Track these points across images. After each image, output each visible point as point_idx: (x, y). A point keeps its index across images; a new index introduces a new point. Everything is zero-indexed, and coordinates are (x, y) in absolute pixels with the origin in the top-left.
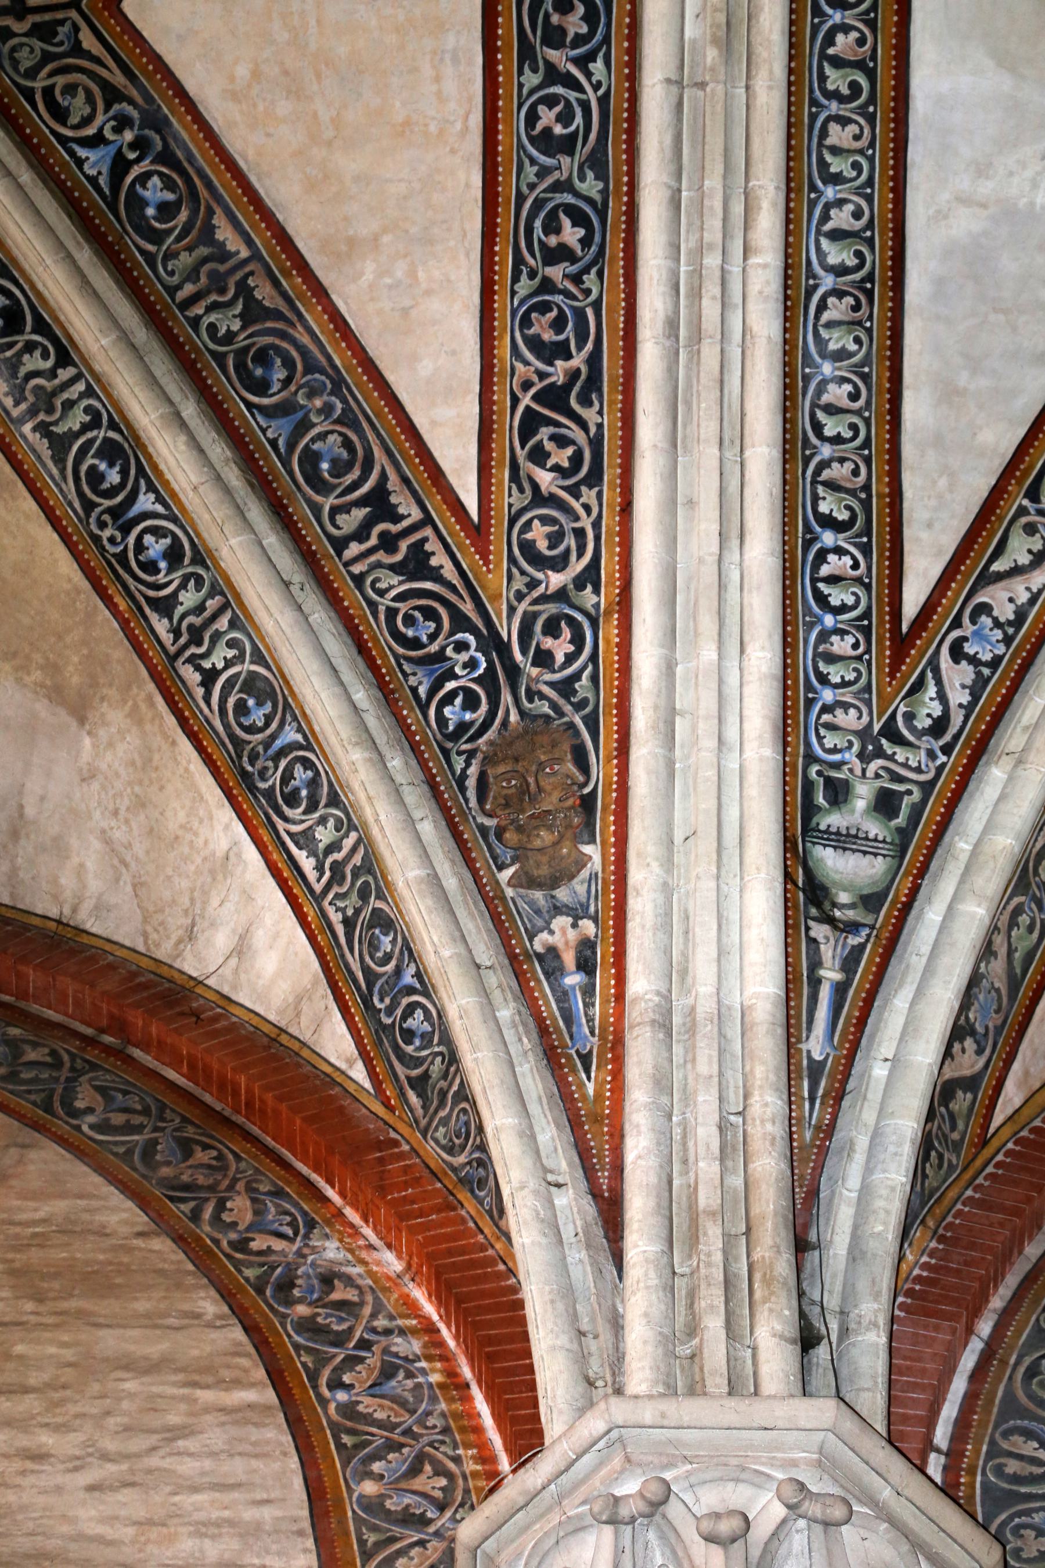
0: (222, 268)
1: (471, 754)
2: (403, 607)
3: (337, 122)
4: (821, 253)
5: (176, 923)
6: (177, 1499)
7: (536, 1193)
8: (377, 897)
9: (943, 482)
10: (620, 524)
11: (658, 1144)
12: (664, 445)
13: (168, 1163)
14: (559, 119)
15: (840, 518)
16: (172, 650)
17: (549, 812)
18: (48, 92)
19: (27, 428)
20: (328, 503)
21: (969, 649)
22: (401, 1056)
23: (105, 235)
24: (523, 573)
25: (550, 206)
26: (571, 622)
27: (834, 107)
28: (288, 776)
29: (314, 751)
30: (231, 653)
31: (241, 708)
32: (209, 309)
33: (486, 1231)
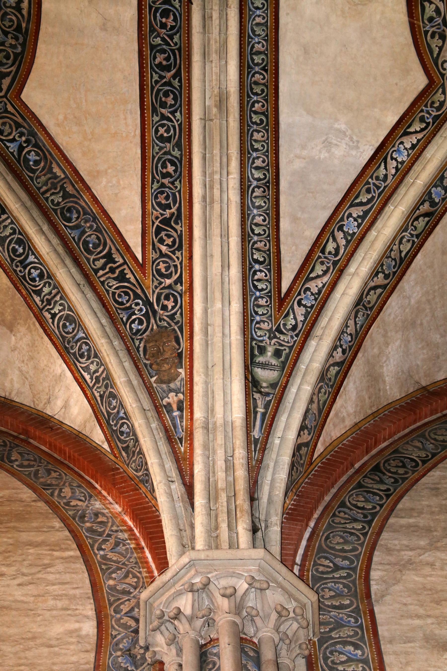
1: (141, 340)
2: (118, 291)
3: (92, 133)
4: (252, 175)
5: (44, 398)
6: (47, 588)
7: (165, 484)
8: (111, 388)
9: (294, 248)
10: (189, 263)
11: (205, 467)
12: (202, 237)
13: (43, 477)
14: (166, 131)
15: (261, 260)
16: (41, 307)
17: (167, 358)
20: (92, 258)
21: (304, 302)
22: (120, 440)
23: (16, 171)
24: (157, 279)
25: (163, 159)
26: (173, 295)
27: (255, 127)
29: (89, 340)
30: (61, 308)
31: (64, 326)
32: (51, 195)
33: (149, 497)
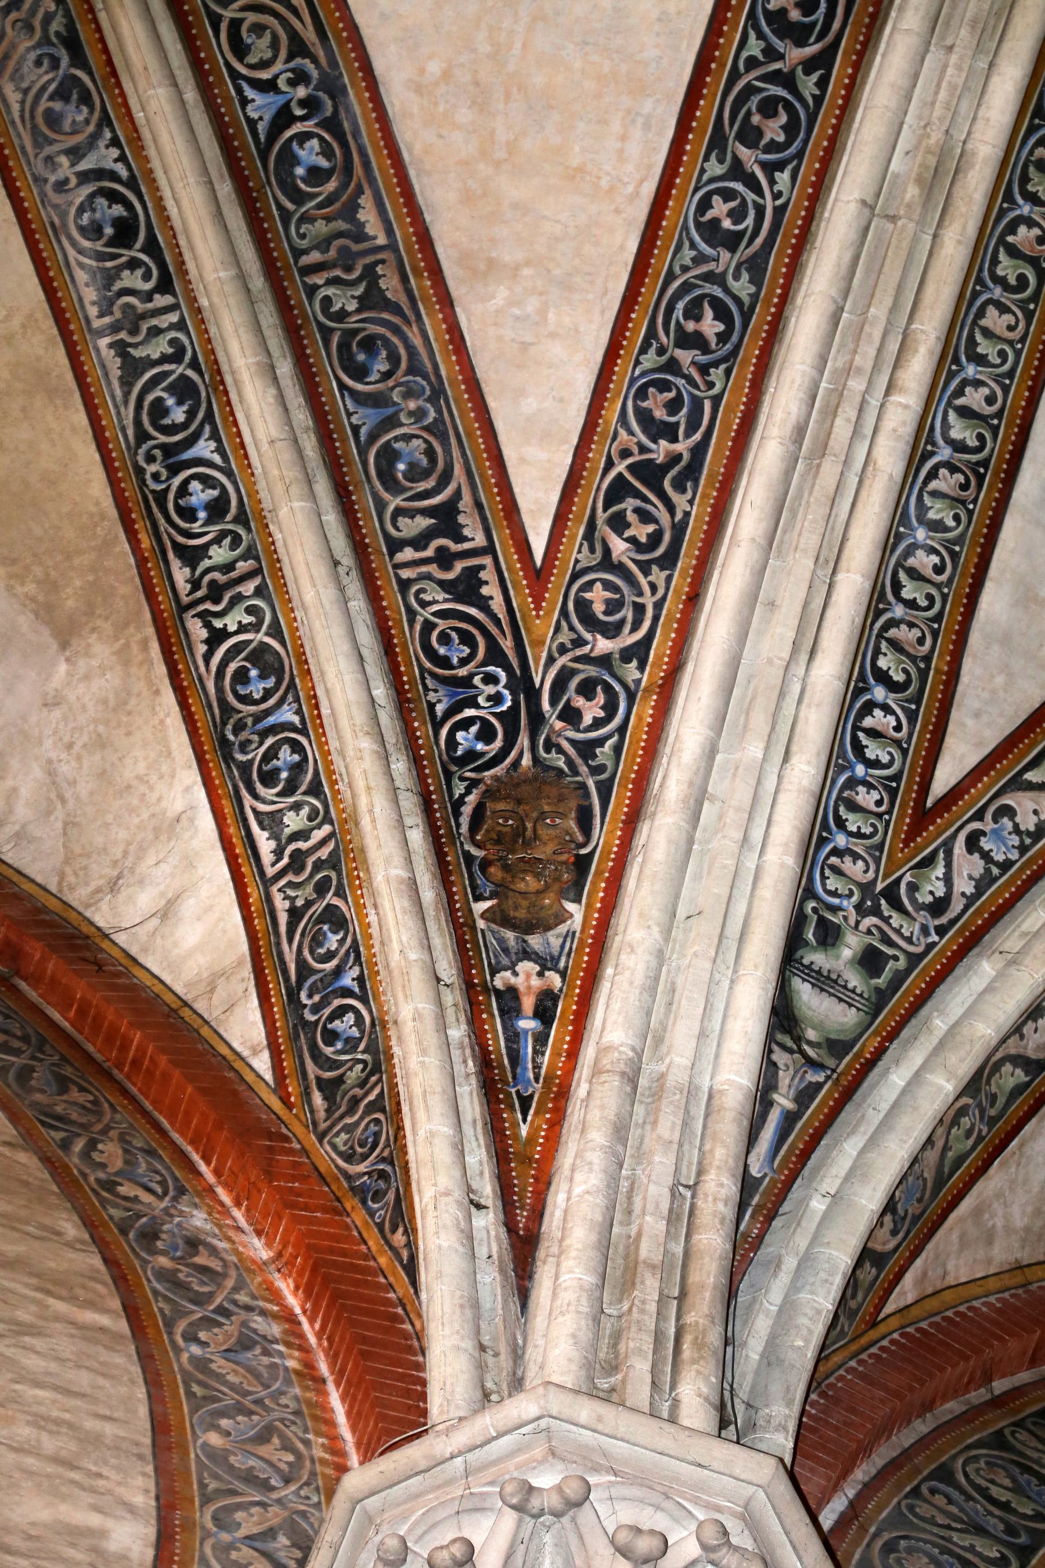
0: (355, 247)
1: (473, 784)
2: (442, 624)
3: (511, 147)
4: (946, 425)
5: (100, 872)
6: (18, 1387)
7: (459, 1203)
8: (337, 894)
9: (1000, 680)
10: (682, 612)
11: (608, 1186)
12: (763, 542)
13: (43, 1092)
14: (731, 214)
15: (896, 678)
17: (540, 860)
18: (235, 25)
19: (104, 342)
20: (394, 502)
21: (985, 844)
22: (317, 1056)
23: (247, 179)
24: (572, 628)
25: (698, 292)
26: (608, 689)
27: (997, 292)
28: (271, 754)
29: (308, 736)
30: (247, 619)
31: (241, 676)
32: (330, 282)
33: (371, 1243)
